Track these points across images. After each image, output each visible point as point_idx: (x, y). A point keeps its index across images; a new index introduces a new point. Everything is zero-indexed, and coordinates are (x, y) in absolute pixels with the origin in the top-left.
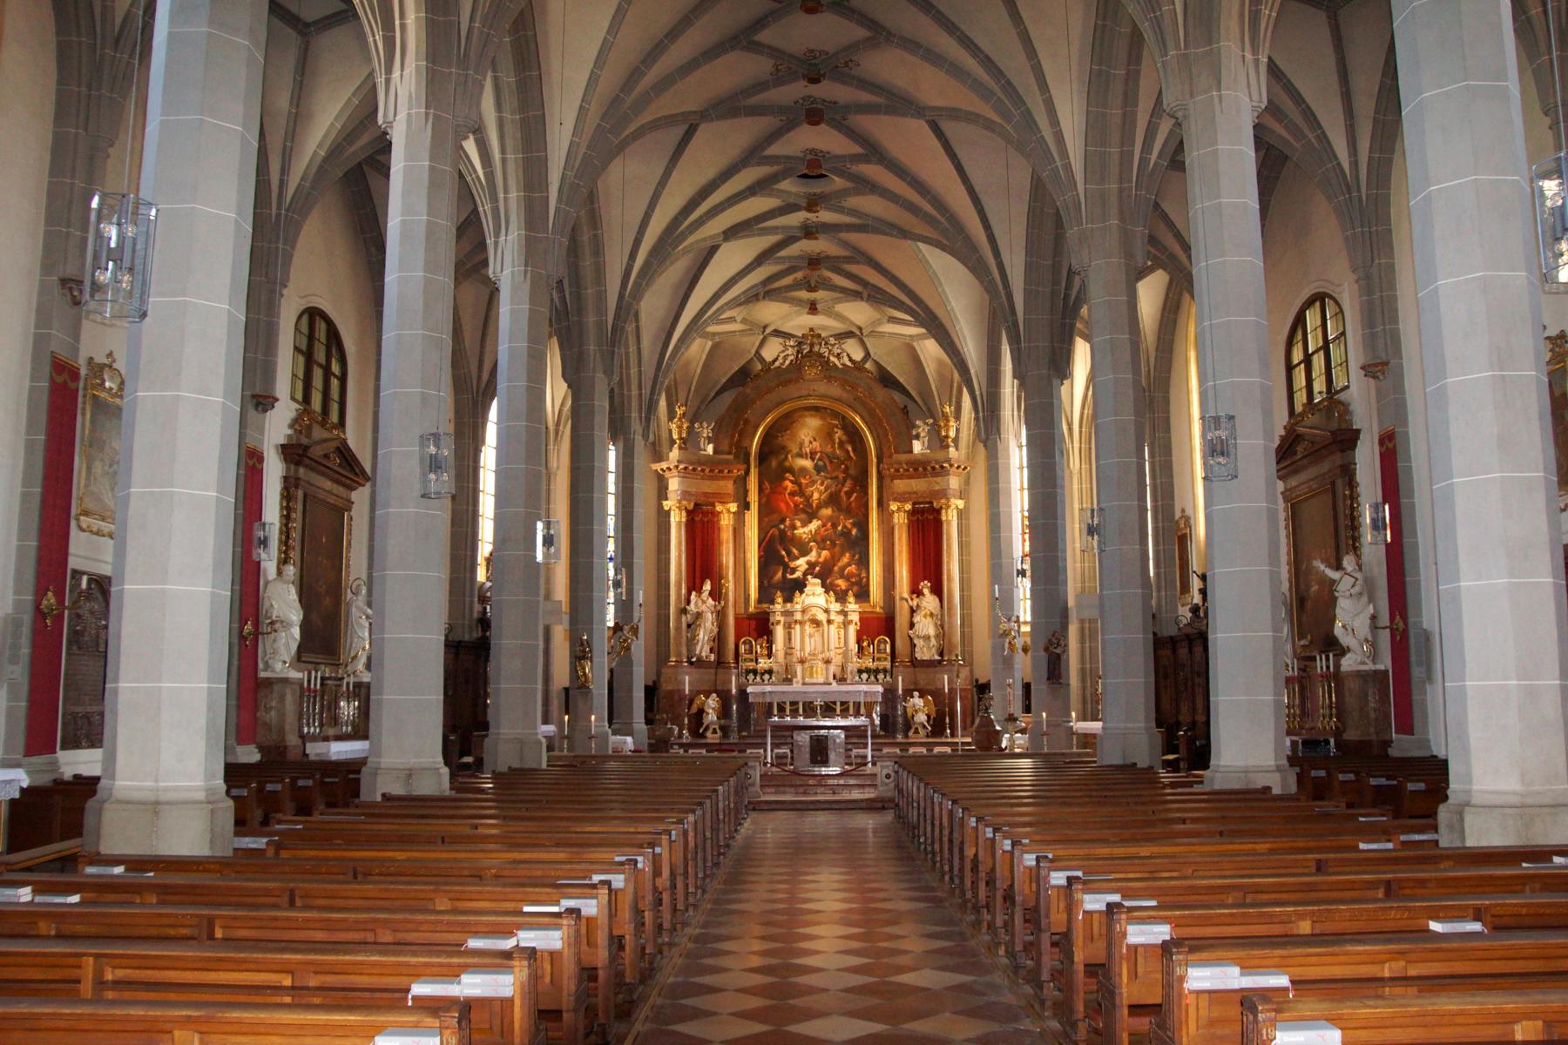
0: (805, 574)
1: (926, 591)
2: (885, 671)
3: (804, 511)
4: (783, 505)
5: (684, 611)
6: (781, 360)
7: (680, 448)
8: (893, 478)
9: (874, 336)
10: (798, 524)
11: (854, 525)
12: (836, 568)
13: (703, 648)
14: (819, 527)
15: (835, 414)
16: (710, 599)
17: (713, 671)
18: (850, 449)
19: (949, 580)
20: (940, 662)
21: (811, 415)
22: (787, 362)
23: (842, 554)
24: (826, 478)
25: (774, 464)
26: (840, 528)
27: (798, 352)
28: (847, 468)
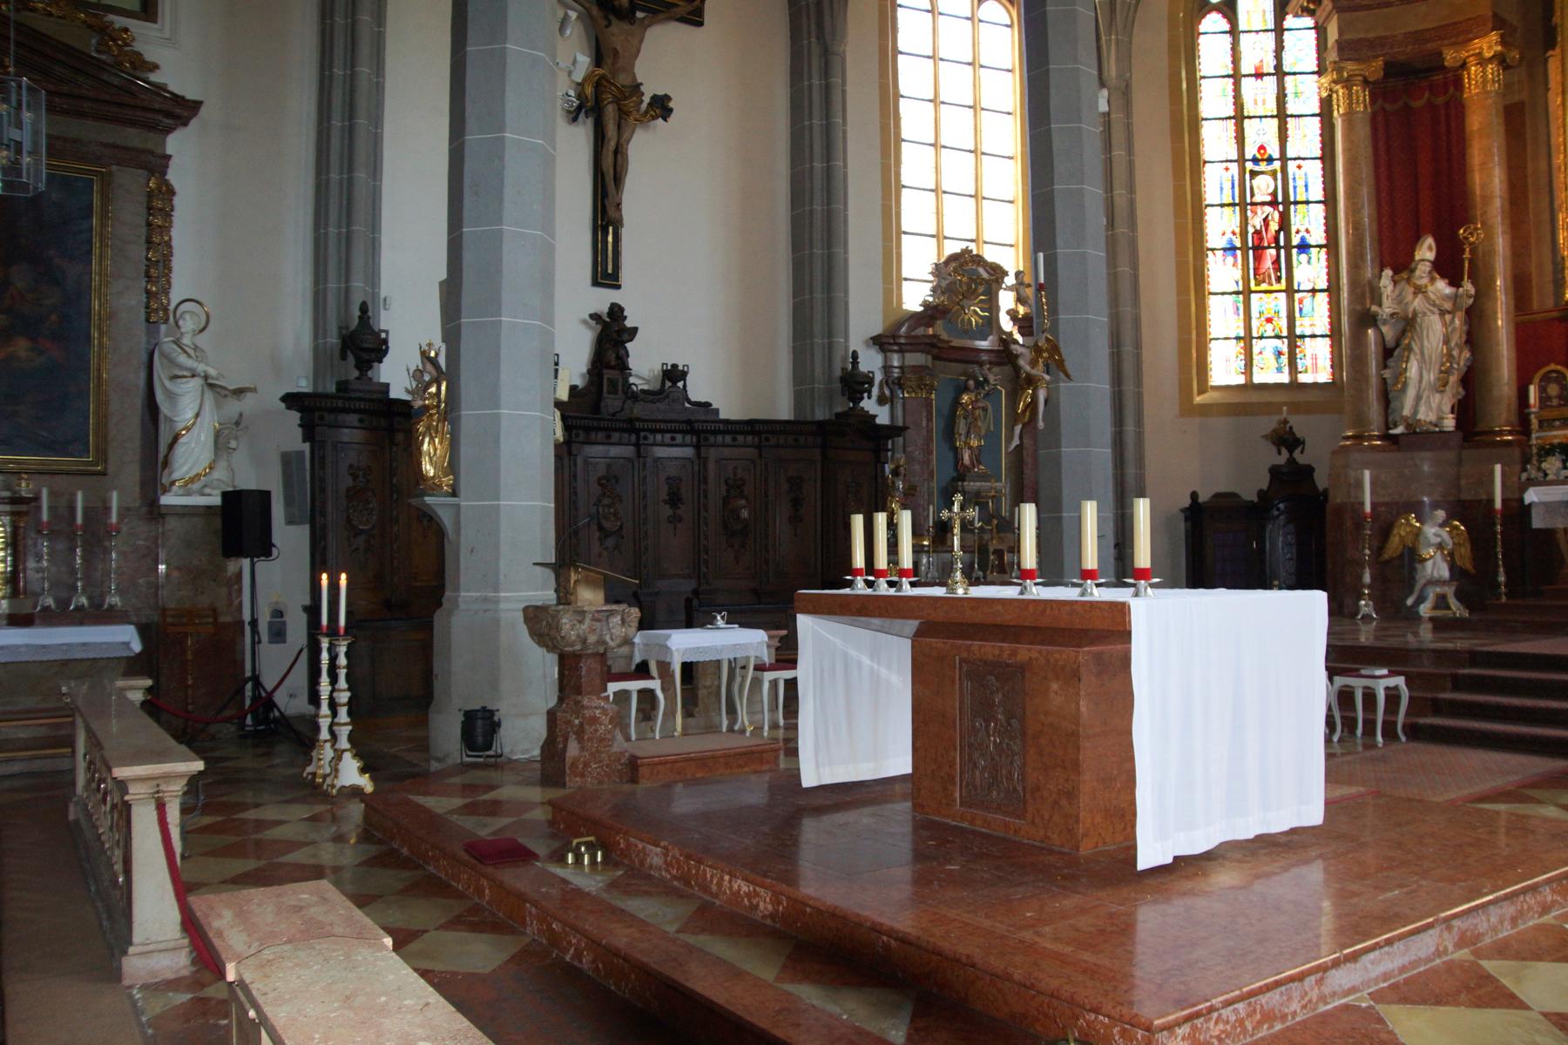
17: (1451, 455)
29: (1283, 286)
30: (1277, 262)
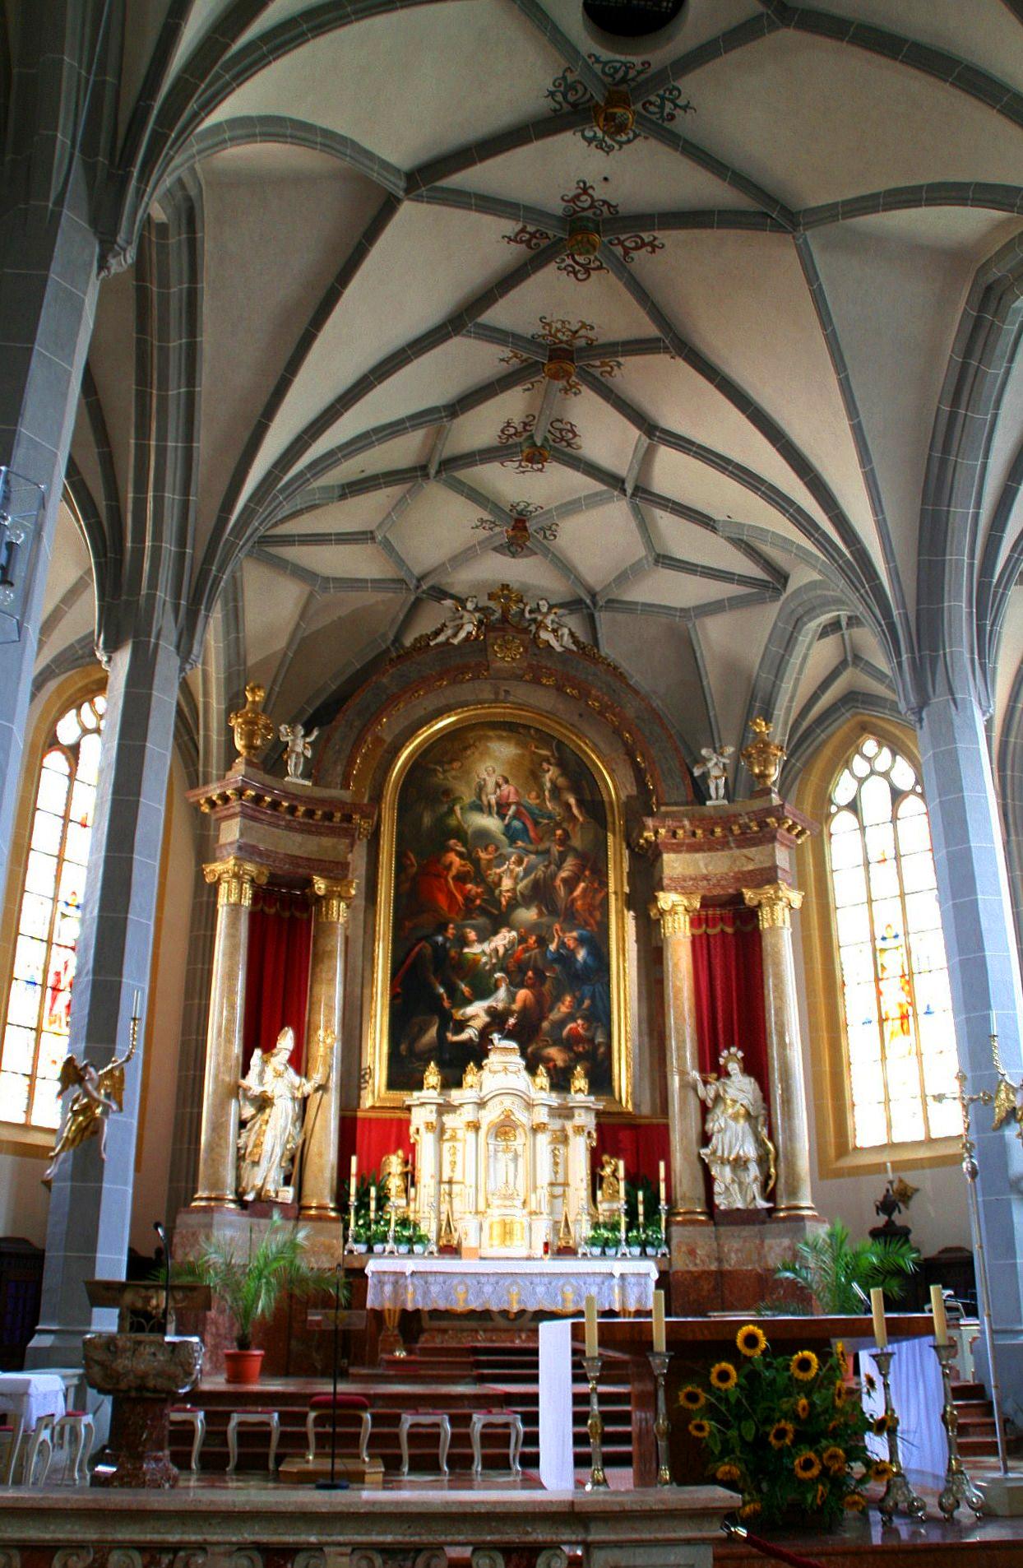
0: (484, 1033)
1: (734, 1068)
3: (483, 911)
4: (443, 902)
5: (236, 1091)
6: (449, 632)
7: (249, 763)
9: (614, 610)
10: (472, 935)
11: (581, 941)
12: (545, 1025)
13: (267, 1176)
14: (512, 943)
15: (545, 739)
16: (291, 1071)
18: (572, 801)
19: (783, 1045)
20: (770, 1211)
21: (501, 738)
22: (462, 635)
23: (558, 999)
24: (528, 852)
25: (427, 820)
26: (553, 947)
27: (480, 622)
28: (567, 835)
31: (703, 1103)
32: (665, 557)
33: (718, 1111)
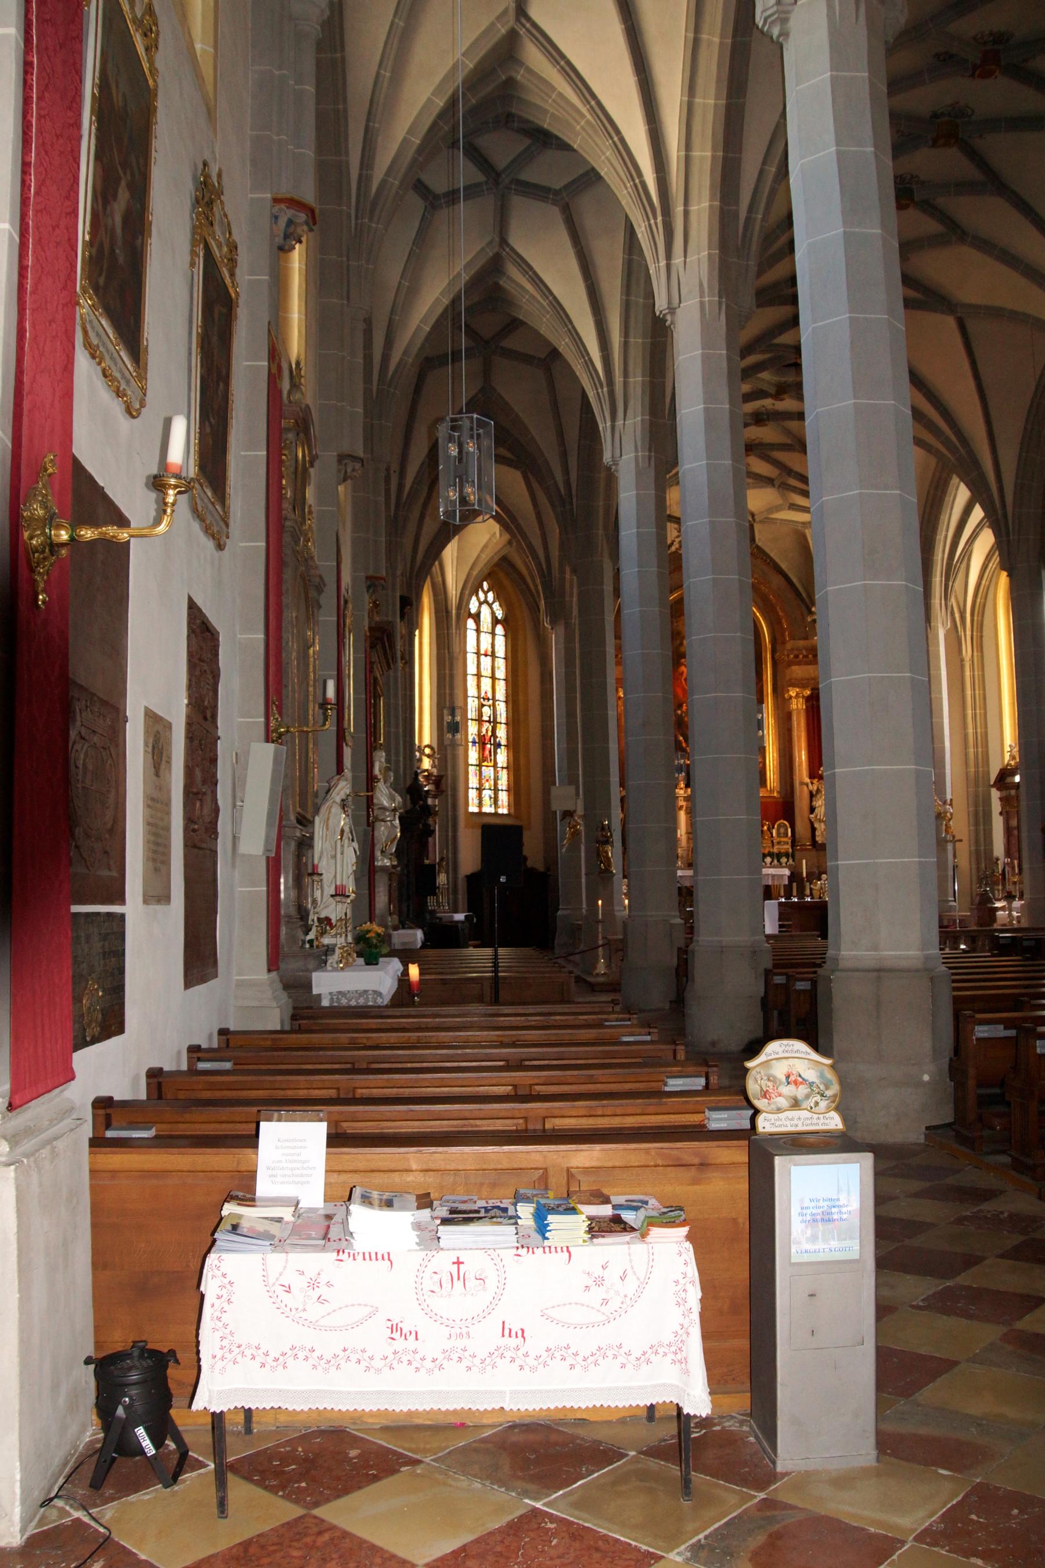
2: (787, 855)
8: (790, 664)
29: (492, 764)
30: (490, 751)
31: (811, 793)
32: (794, 505)
33: (818, 796)
